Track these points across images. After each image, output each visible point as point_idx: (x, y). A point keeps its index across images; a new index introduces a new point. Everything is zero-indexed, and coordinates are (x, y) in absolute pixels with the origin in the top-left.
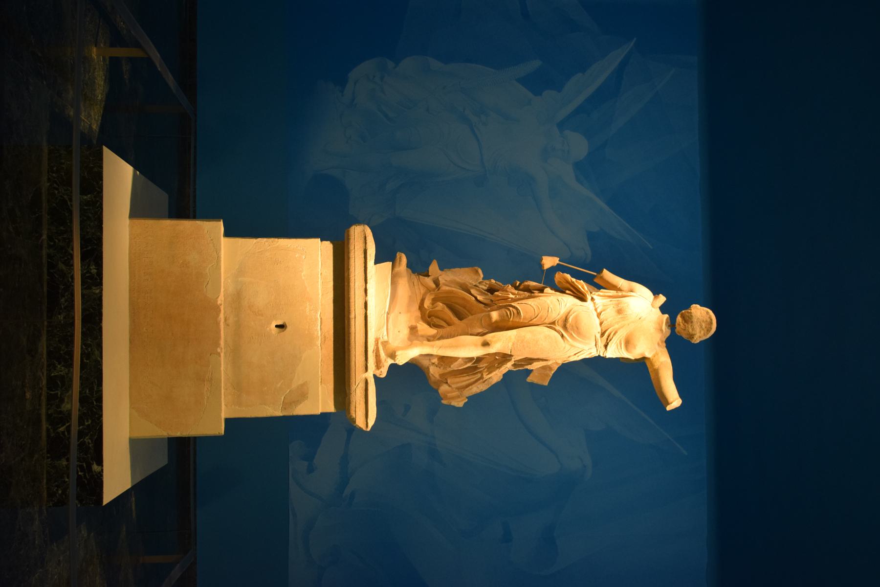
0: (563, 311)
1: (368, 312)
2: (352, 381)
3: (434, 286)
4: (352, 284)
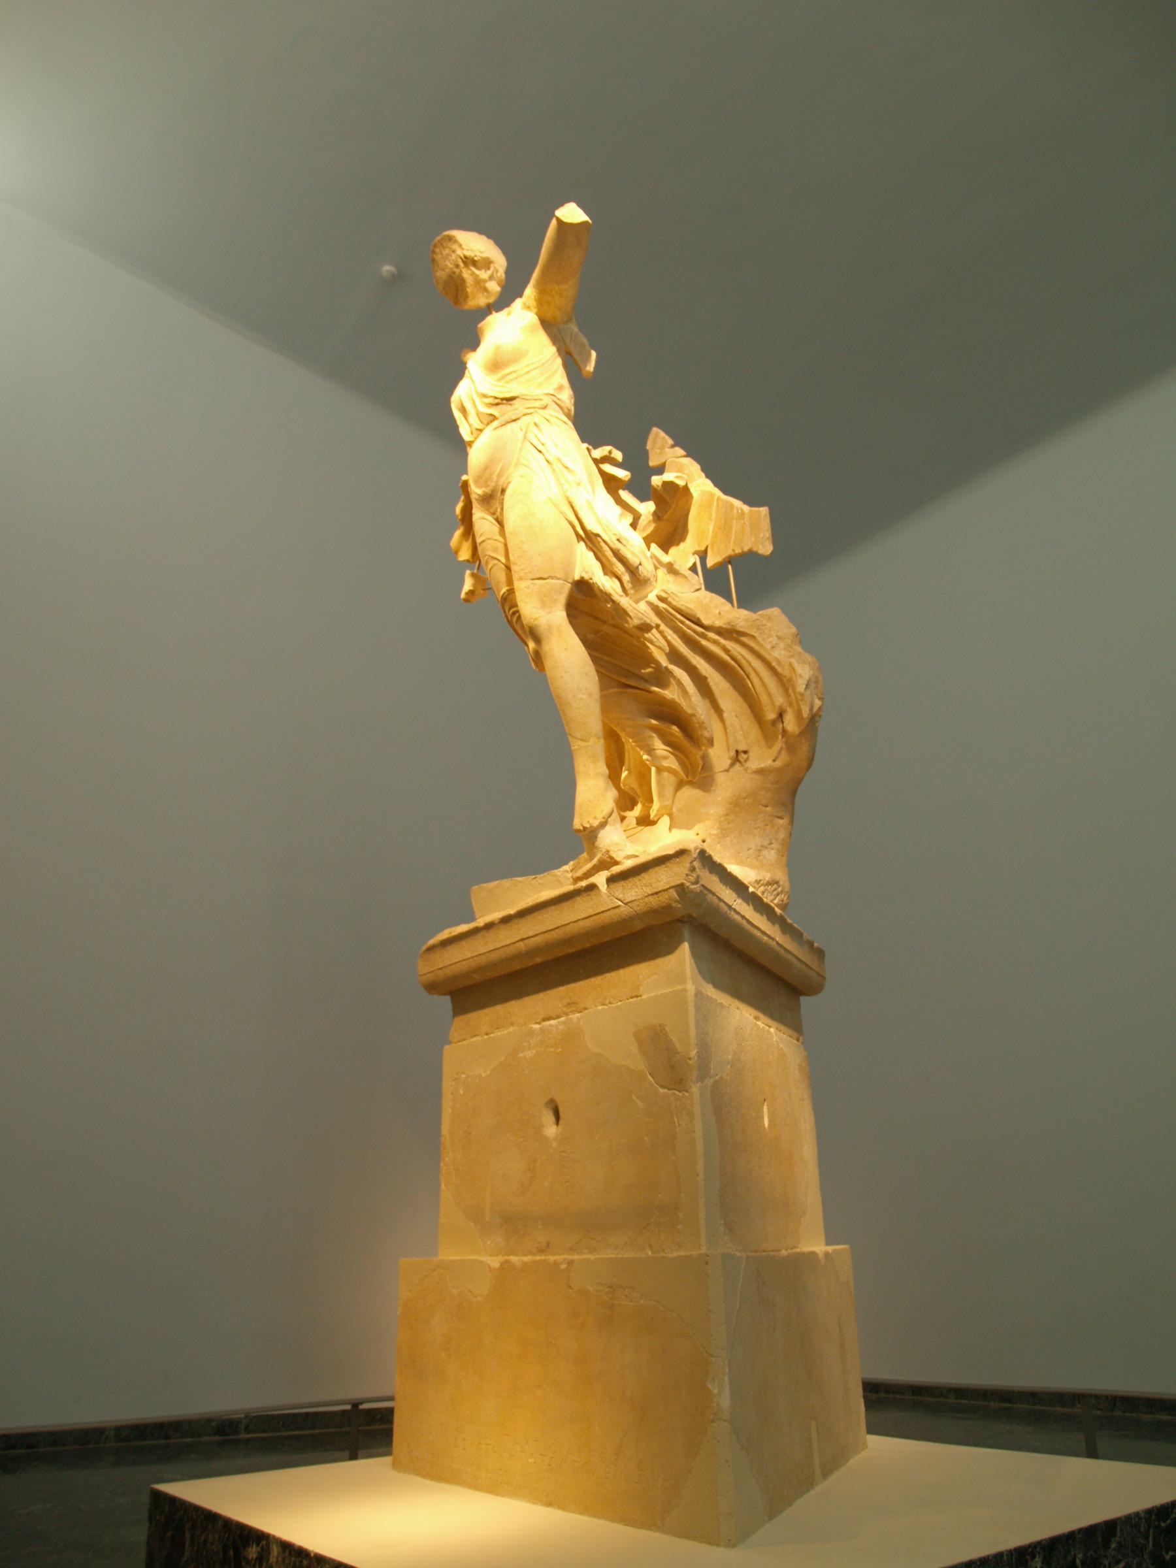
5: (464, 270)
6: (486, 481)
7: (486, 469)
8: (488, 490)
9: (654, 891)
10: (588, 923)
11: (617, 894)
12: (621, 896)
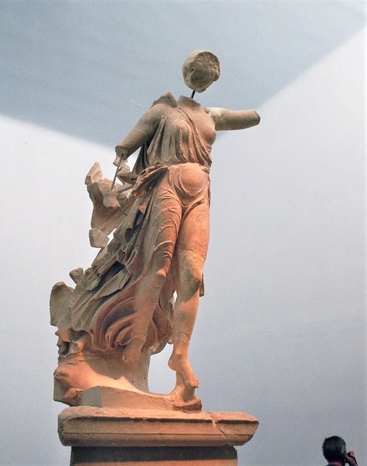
0: (175, 196)
1: (158, 417)
2: (217, 438)
4: (128, 437)
8: (191, 194)
9: (240, 433)
10: (204, 438)
11: (221, 429)
12: (223, 430)
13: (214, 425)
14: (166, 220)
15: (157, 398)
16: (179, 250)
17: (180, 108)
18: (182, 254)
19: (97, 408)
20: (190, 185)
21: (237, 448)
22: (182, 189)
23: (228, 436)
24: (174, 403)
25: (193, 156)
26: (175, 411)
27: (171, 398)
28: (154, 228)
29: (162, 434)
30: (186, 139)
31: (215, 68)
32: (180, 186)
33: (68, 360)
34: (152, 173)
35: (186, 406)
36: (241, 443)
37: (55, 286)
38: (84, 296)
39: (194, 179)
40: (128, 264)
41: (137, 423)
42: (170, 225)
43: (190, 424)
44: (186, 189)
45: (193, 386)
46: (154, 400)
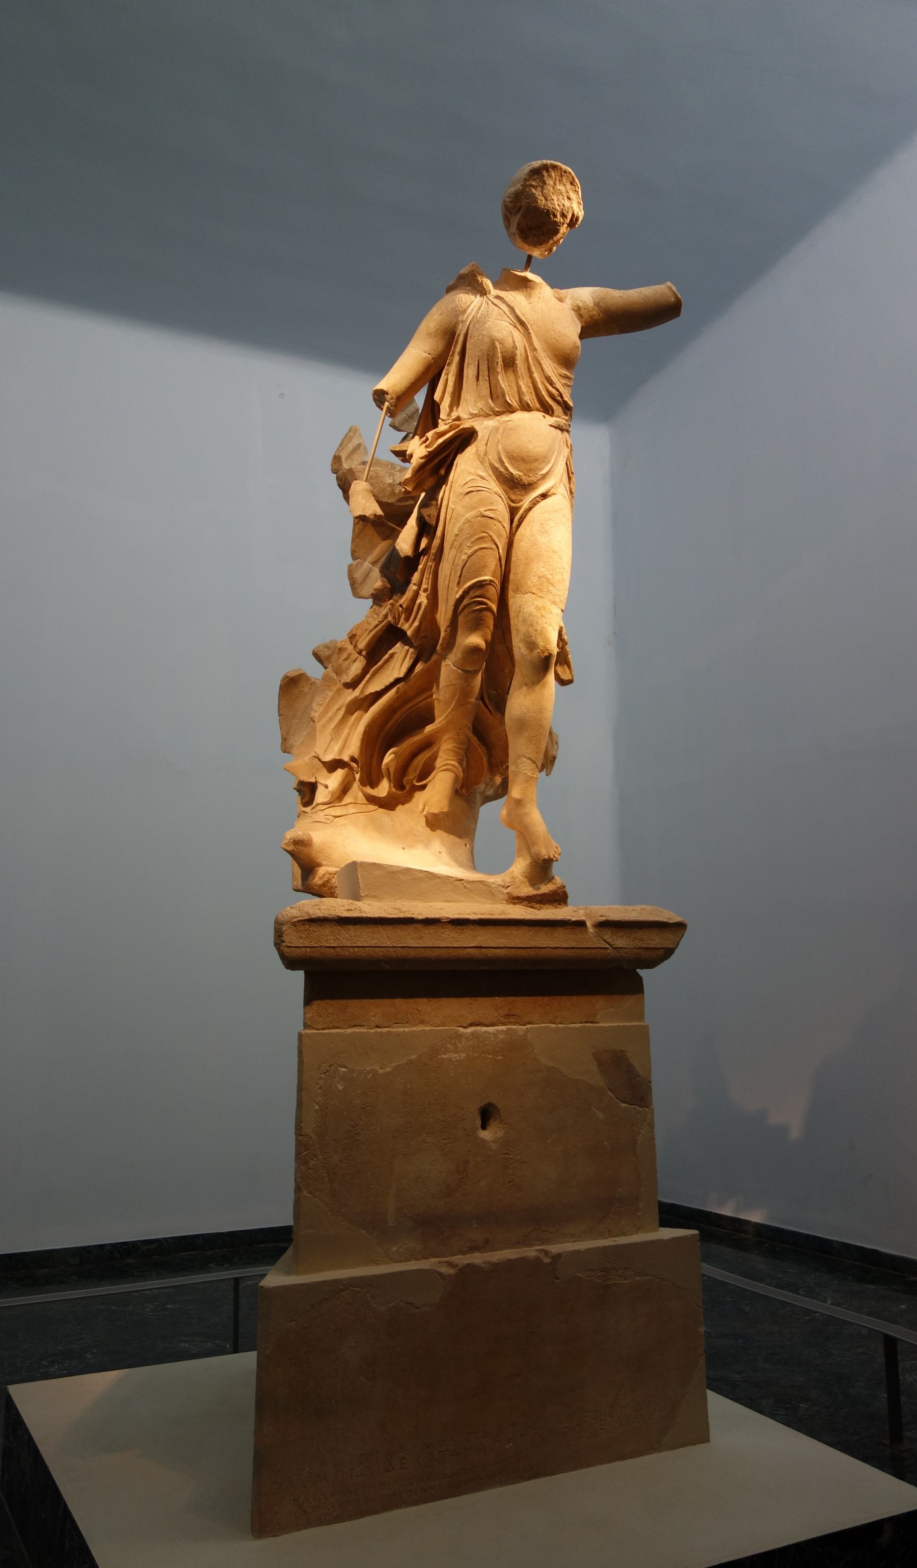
0: (493, 485)
1: (472, 917)
3: (340, 773)
4: (413, 953)
5: (565, 225)
6: (530, 470)
7: (536, 460)
8: (526, 480)
9: (644, 945)
11: (606, 937)
12: (609, 940)
13: (591, 930)
14: (476, 534)
15: (473, 882)
16: (511, 593)
17: (498, 297)
18: (515, 601)
19: (351, 901)
20: (523, 459)
21: (642, 972)
22: (507, 469)
23: (622, 951)
24: (509, 890)
25: (530, 398)
26: (512, 906)
27: (503, 881)
28: (454, 552)
29: (481, 947)
30: (510, 363)
31: (569, 198)
32: (502, 463)
33: (313, 816)
34: (441, 441)
35: (534, 896)
36: (651, 964)
37: (286, 677)
38: (338, 693)
39: (530, 447)
40: (411, 626)
41: (430, 927)
42: (485, 546)
43: (538, 928)
44: (515, 468)
45: (547, 857)
46: (466, 884)
